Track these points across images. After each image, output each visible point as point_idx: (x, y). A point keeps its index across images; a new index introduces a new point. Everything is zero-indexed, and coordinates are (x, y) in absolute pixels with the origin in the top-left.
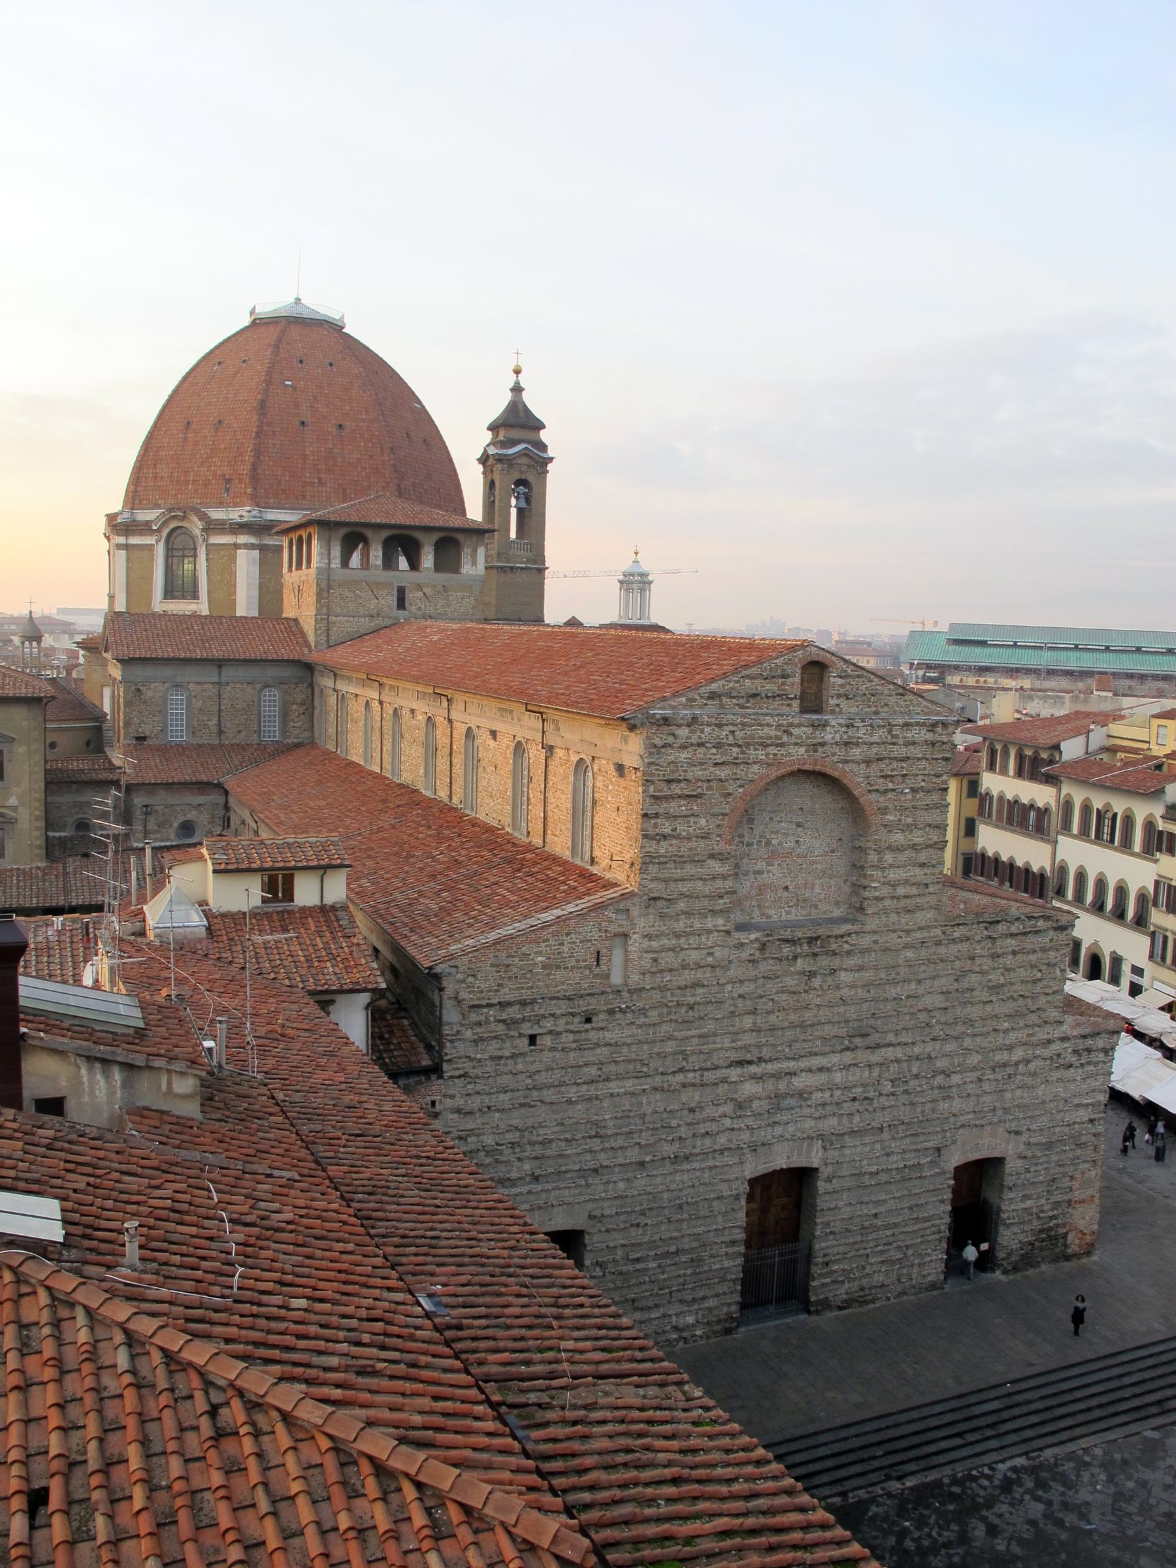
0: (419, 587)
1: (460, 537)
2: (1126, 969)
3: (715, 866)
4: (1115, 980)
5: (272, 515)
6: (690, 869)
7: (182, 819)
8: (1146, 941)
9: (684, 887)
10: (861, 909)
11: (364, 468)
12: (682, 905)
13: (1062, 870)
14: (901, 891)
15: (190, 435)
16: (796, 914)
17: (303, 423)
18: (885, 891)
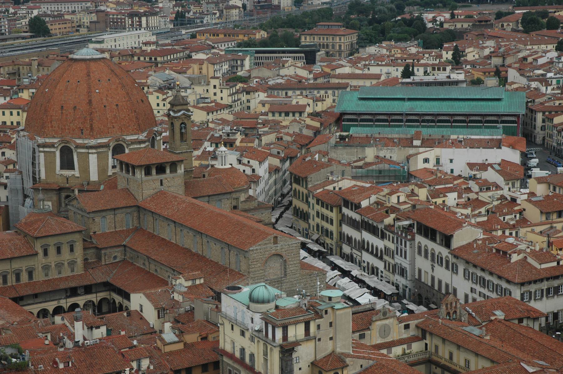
0: (166, 179)
1: (177, 163)
2: (379, 271)
3: (261, 271)
4: (377, 275)
5: (100, 141)
6: (257, 272)
7: (114, 255)
8: (383, 264)
9: (257, 275)
10: (286, 275)
11: (127, 120)
12: (256, 278)
13: (364, 241)
14: (293, 271)
15: (64, 112)
16: (275, 277)
17: (105, 106)
18: (290, 272)
